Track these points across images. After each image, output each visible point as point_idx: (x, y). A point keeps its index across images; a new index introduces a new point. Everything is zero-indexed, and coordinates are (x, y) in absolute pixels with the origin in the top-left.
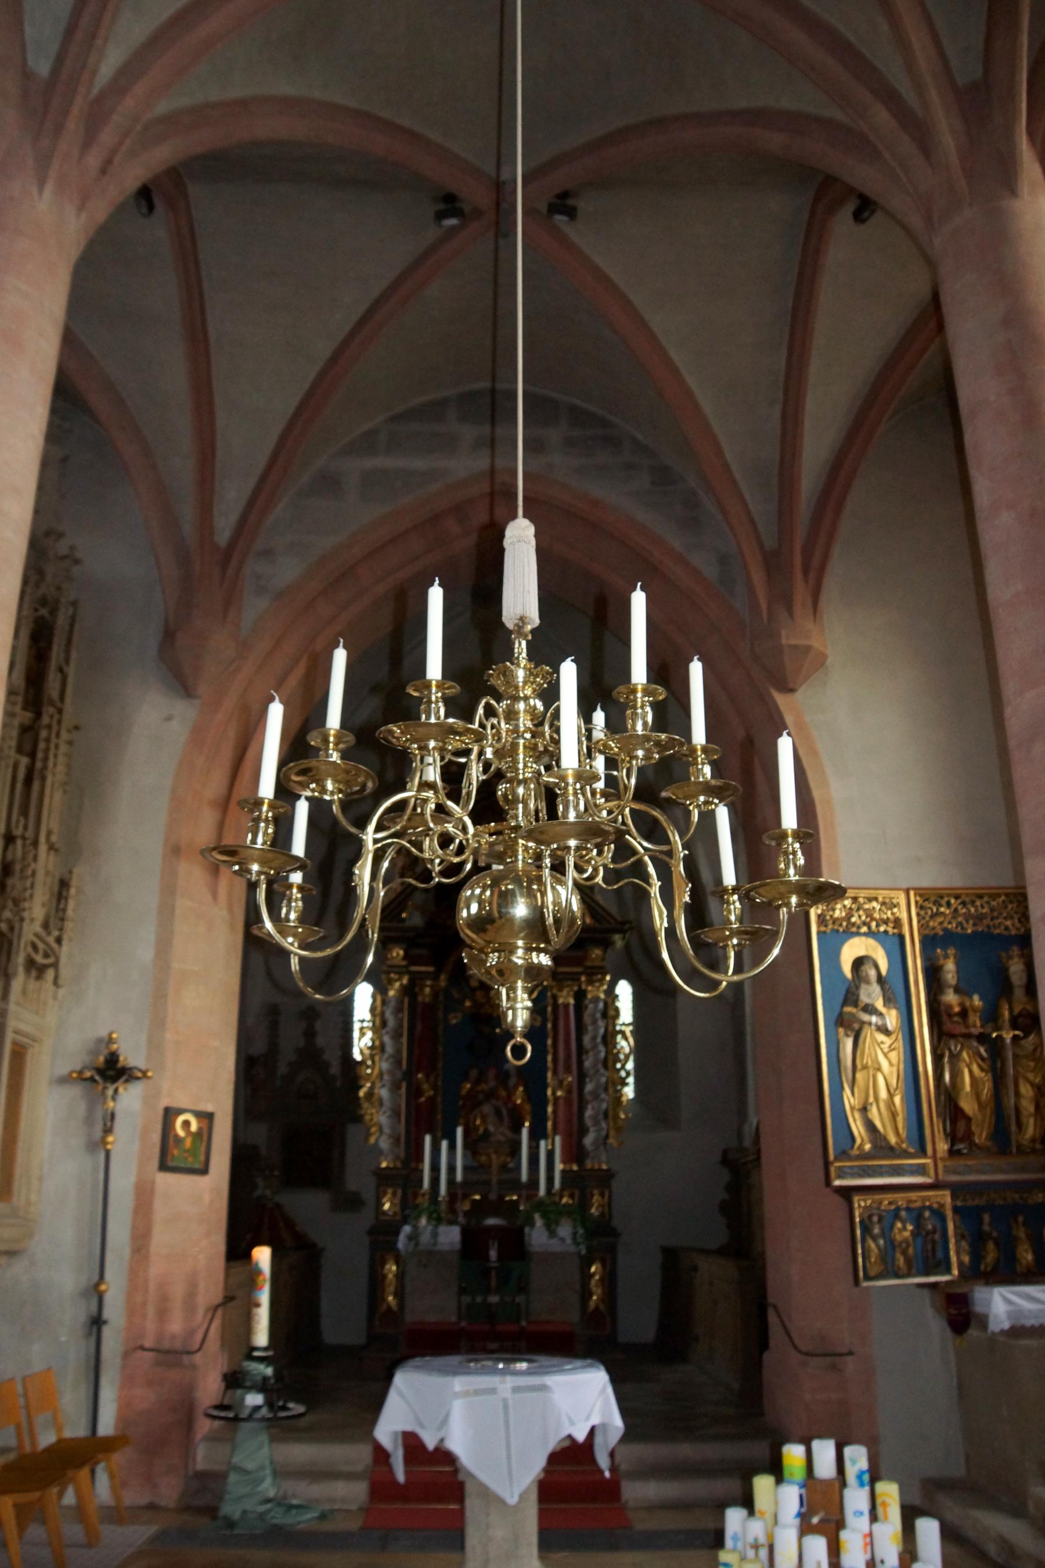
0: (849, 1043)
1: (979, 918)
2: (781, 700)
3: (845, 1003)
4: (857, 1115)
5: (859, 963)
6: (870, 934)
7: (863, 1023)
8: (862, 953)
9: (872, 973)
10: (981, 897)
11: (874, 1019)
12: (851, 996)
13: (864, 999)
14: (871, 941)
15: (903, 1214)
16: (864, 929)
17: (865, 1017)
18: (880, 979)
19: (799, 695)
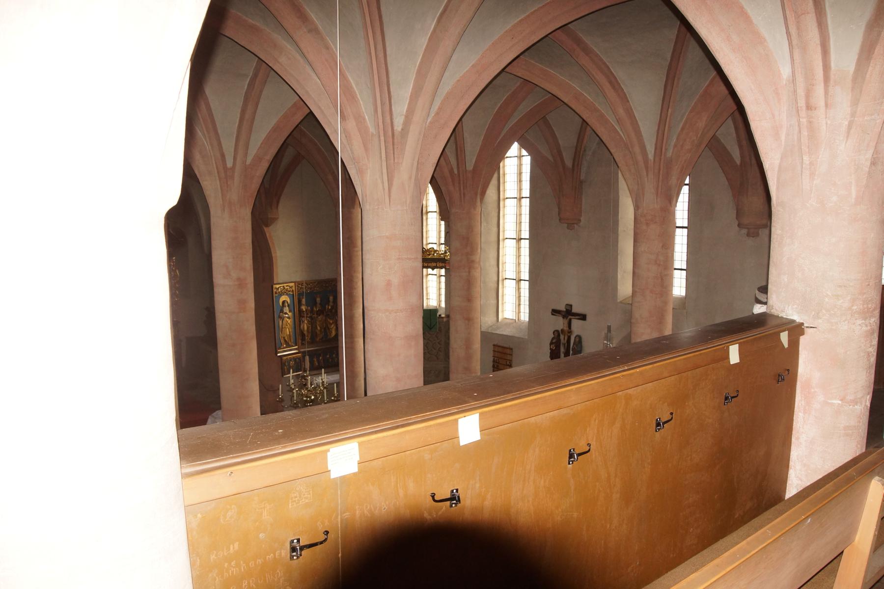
0: (281, 322)
1: (311, 288)
2: (266, 229)
3: (280, 313)
4: (283, 338)
5: (284, 302)
6: (287, 295)
7: (284, 317)
8: (284, 299)
9: (287, 304)
10: (312, 283)
11: (287, 315)
12: (282, 311)
13: (285, 311)
14: (286, 296)
15: (292, 360)
16: (285, 294)
17: (285, 315)
18: (288, 306)
19: (271, 227)
